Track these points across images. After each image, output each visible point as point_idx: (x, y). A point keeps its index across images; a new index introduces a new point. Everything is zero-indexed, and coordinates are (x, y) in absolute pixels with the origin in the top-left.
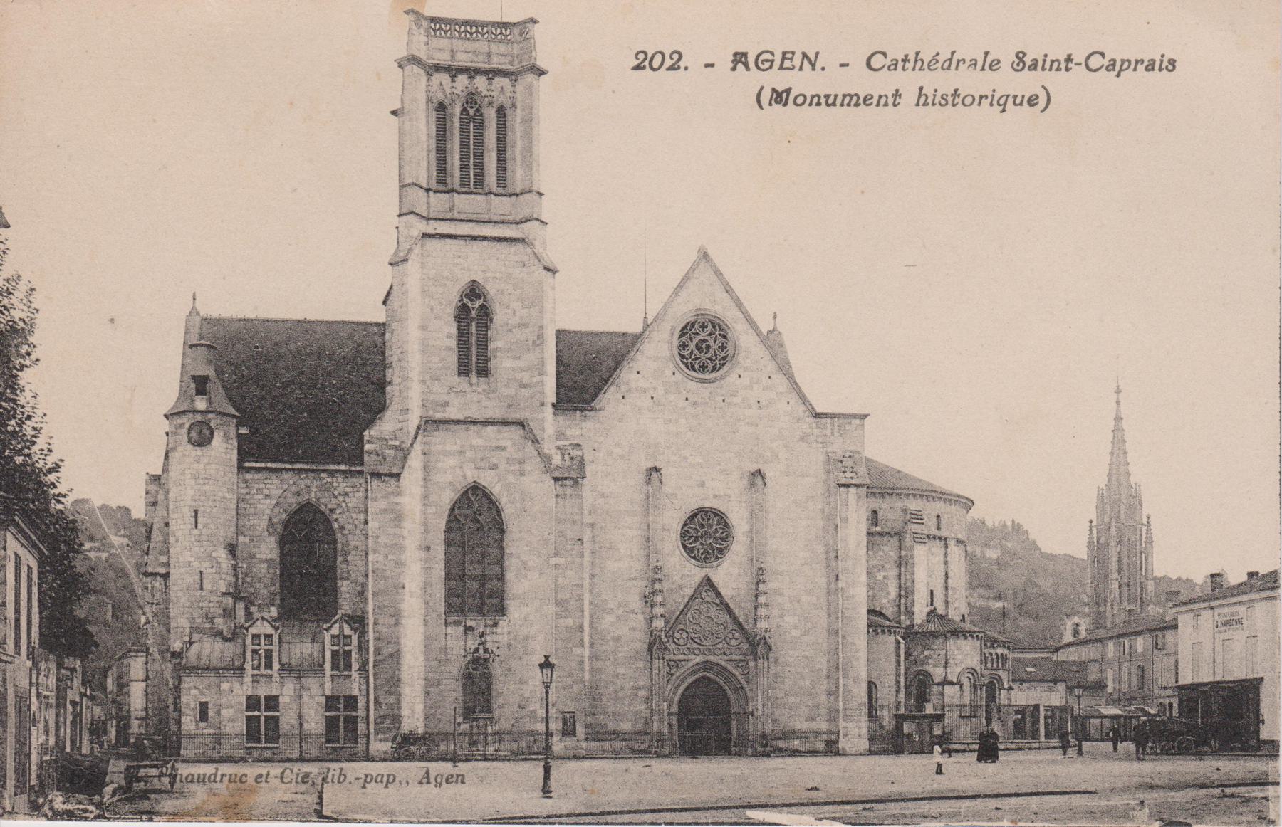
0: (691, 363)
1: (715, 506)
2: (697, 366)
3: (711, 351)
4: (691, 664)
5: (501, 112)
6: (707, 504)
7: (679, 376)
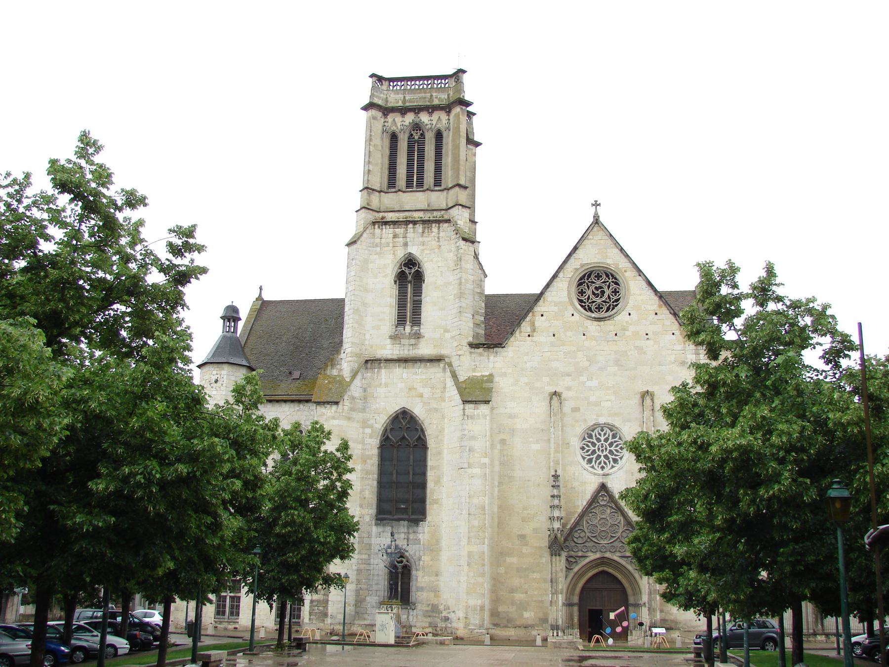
1: (610, 422)
2: (593, 308)
3: (606, 295)
4: (587, 560)
5: (439, 136)
6: (602, 420)
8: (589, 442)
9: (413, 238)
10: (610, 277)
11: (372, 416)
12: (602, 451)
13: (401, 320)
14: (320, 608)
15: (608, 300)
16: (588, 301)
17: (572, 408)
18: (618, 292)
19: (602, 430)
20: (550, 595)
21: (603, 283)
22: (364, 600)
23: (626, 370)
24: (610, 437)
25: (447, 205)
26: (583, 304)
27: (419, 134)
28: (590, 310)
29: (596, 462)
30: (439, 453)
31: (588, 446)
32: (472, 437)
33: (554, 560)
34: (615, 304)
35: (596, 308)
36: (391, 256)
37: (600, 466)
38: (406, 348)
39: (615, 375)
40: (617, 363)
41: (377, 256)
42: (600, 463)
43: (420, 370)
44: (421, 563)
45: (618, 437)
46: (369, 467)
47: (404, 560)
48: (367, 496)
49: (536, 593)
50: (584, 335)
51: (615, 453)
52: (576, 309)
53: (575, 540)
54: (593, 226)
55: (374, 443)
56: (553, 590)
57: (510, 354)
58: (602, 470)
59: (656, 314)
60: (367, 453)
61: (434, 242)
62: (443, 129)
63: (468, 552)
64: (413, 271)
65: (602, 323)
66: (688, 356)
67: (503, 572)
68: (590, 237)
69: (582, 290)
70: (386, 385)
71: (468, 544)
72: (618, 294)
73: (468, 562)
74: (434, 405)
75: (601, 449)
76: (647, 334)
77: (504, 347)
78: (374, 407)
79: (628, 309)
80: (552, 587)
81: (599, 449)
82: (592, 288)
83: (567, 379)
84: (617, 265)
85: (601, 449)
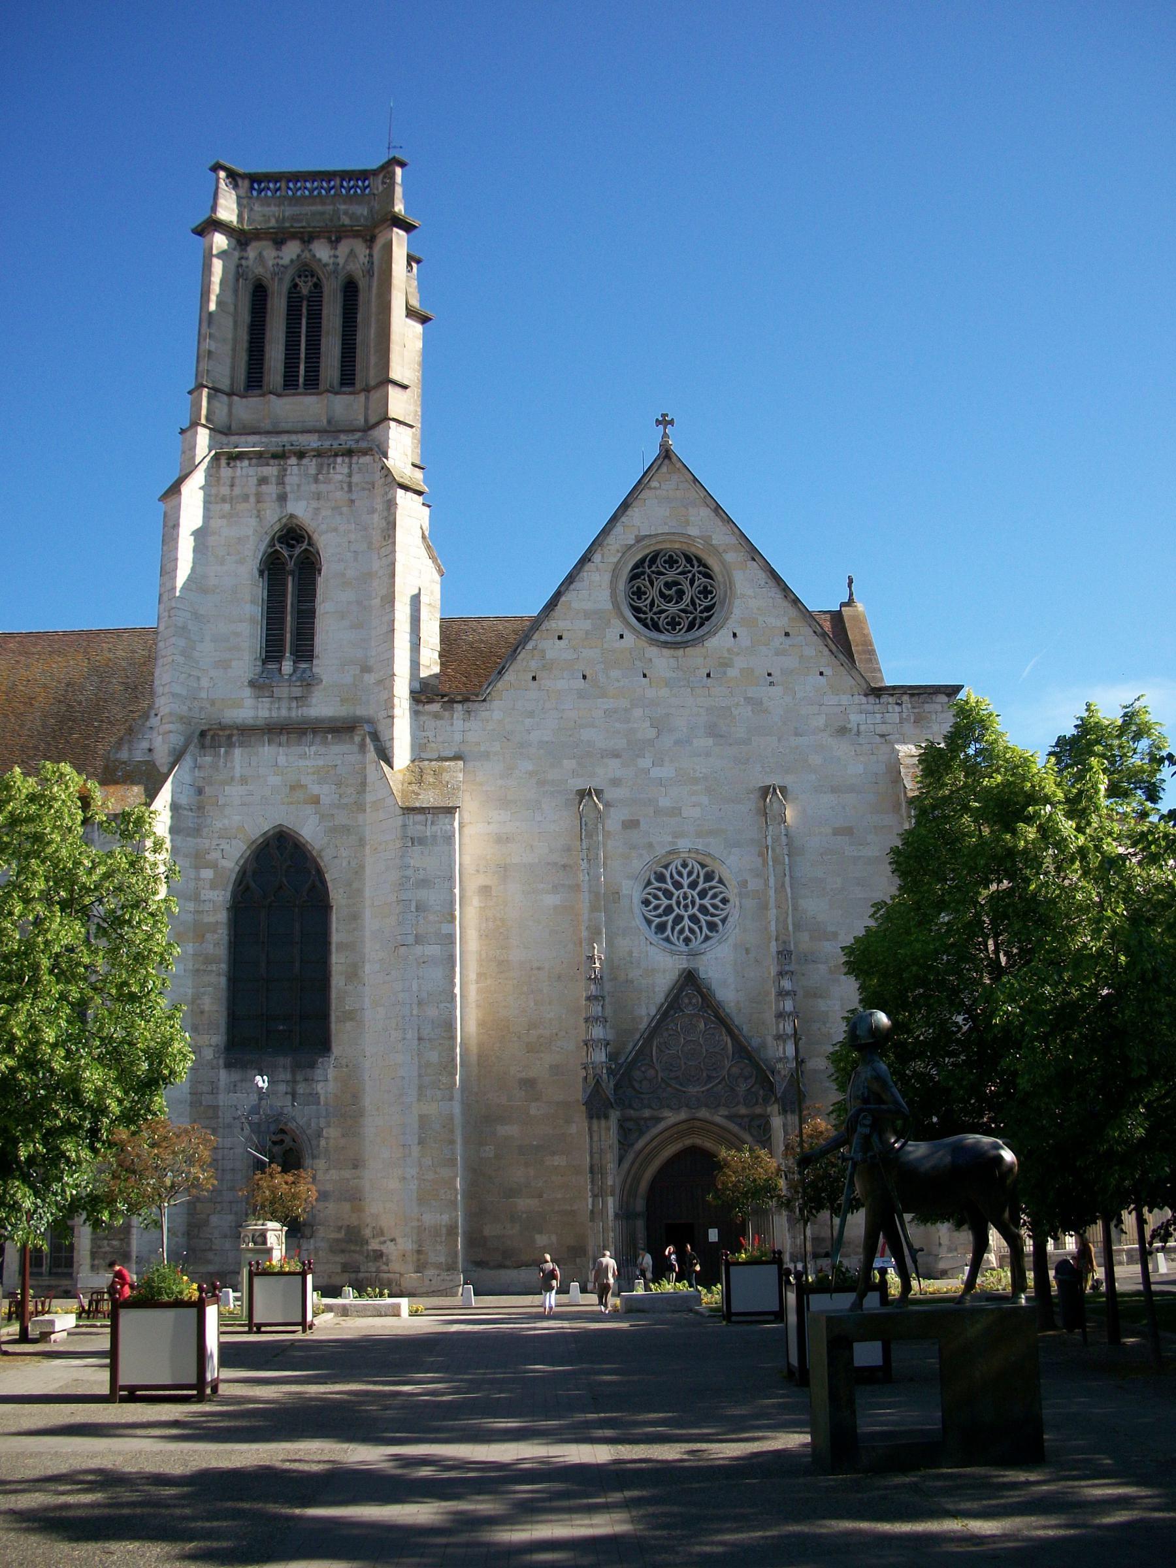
0: (652, 619)
2: (661, 623)
3: (687, 599)
4: (662, 1126)
5: (351, 290)
7: (629, 638)
8: (659, 889)
9: (299, 486)
10: (695, 562)
11: (215, 842)
12: (686, 906)
13: (272, 651)
14: (115, 1243)
15: (691, 608)
16: (651, 610)
18: (711, 592)
20: (590, 1200)
21: (680, 574)
22: (206, 1223)
24: (701, 879)
25: (366, 420)
27: (310, 284)
28: (656, 627)
29: (673, 929)
30: (355, 917)
31: (656, 897)
32: (423, 880)
33: (595, 1128)
34: (705, 614)
35: (668, 624)
36: (253, 522)
37: (682, 937)
38: (284, 704)
39: (708, 755)
40: (712, 731)
41: (224, 521)
42: (682, 931)
43: (313, 749)
44: (323, 1143)
46: (210, 948)
47: (287, 1139)
48: (206, 1008)
49: (559, 1196)
50: (645, 676)
51: (712, 910)
52: (628, 624)
53: (637, 1085)
54: (659, 462)
55: (221, 898)
56: (596, 1188)
57: (497, 715)
59: (787, 634)
61: (339, 494)
62: (359, 276)
63: (420, 1116)
64: (297, 551)
65: (680, 652)
66: (853, 717)
67: (491, 1155)
68: (654, 484)
69: (639, 588)
70: (244, 780)
71: (419, 1100)
72: (710, 596)
73: (420, 1137)
74: (342, 818)
76: (769, 675)
77: (484, 700)
78: (219, 825)
79: (732, 625)
80: (592, 1182)
81: (678, 903)
82: (660, 583)
83: (614, 764)
84: (707, 540)
85: (683, 903)
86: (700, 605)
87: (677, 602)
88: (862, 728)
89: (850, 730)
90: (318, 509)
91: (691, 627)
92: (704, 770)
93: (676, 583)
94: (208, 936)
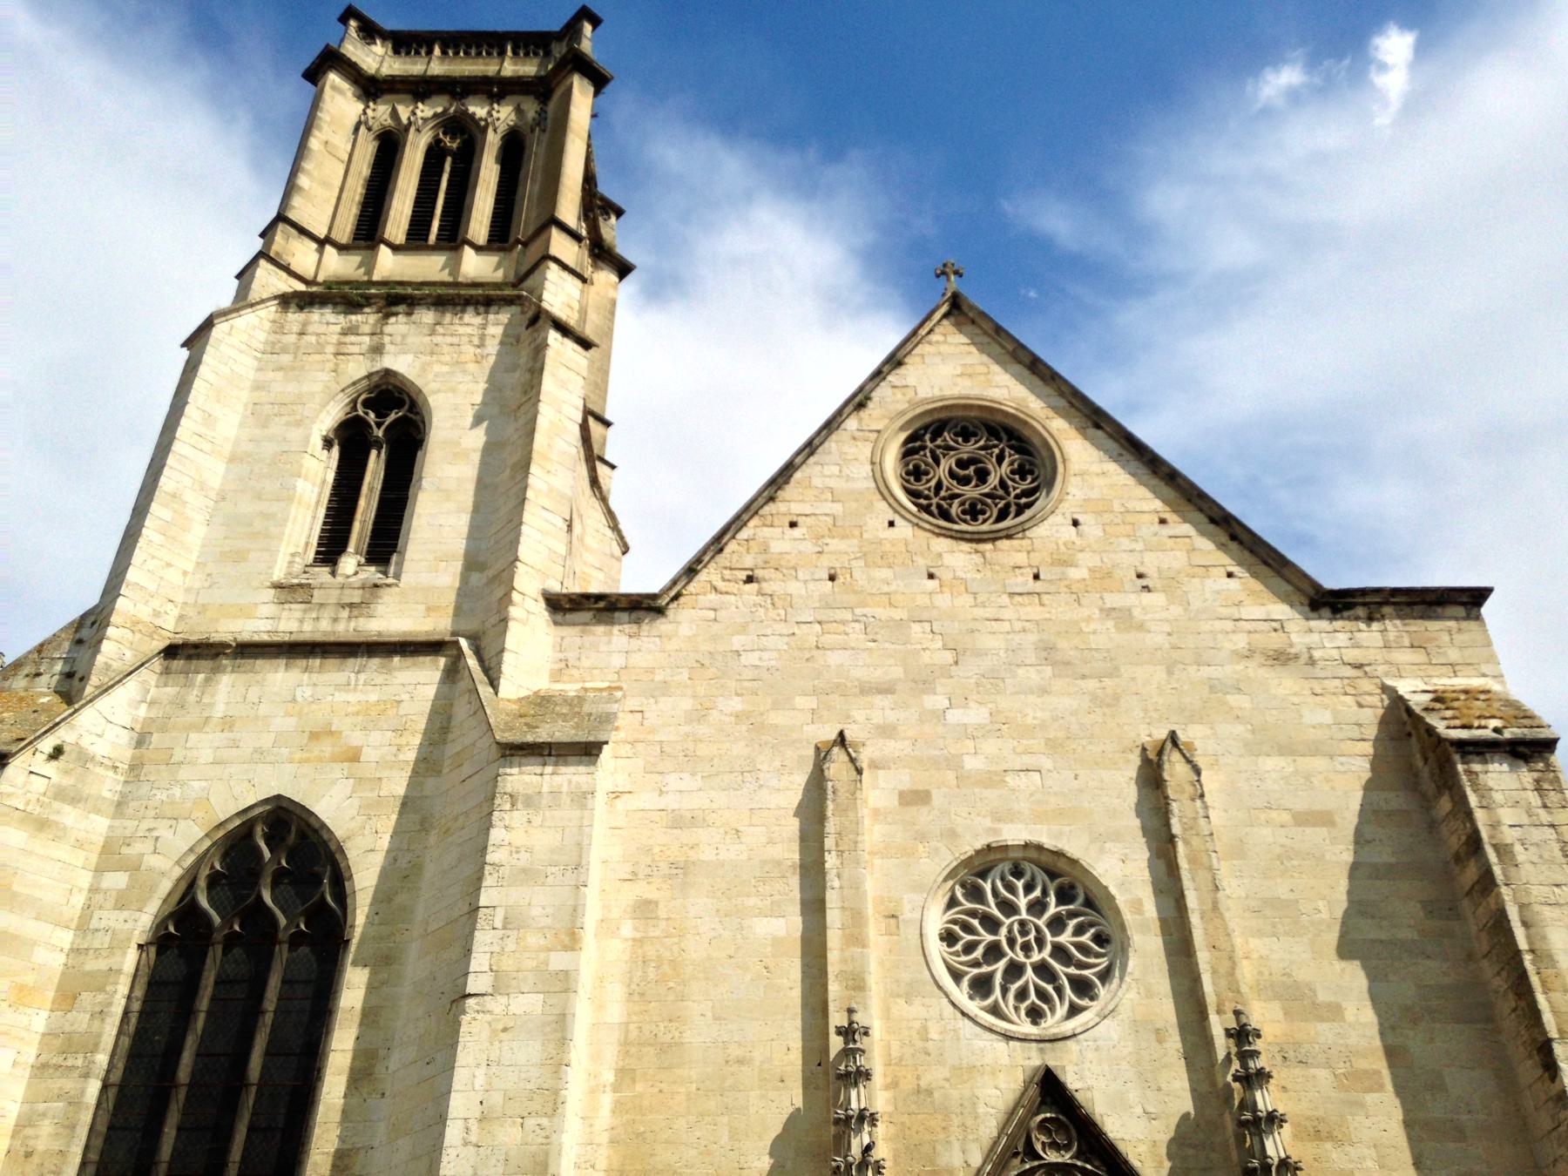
1: (1049, 843)
2: (955, 509)
3: (993, 480)
6: (1014, 834)
7: (904, 530)
8: (973, 914)
9: (404, 337)
10: (1003, 435)
11: (144, 825)
12: (1026, 948)
15: (1001, 492)
17: (902, 794)
19: (1018, 873)
21: (981, 448)
23: (1084, 677)
26: (922, 501)
29: (1005, 991)
31: (968, 929)
32: (524, 871)
34: (1023, 500)
35: (964, 512)
37: (1023, 1006)
40: (1047, 652)
41: (279, 375)
43: (362, 677)
45: (1081, 899)
57: (685, 630)
58: (1035, 1023)
60: (88, 967)
65: (988, 546)
66: (1295, 638)
68: (934, 337)
69: (917, 467)
75: (1020, 940)
76: (1140, 576)
78: (161, 796)
81: (1011, 942)
82: (947, 463)
83: (879, 701)
85: (1020, 940)
86: (1015, 489)
87: (977, 486)
88: (1317, 654)
89: (1297, 657)
90: (430, 364)
91: (1003, 515)
92: (1039, 714)
93: (972, 461)
94: (86, 997)
